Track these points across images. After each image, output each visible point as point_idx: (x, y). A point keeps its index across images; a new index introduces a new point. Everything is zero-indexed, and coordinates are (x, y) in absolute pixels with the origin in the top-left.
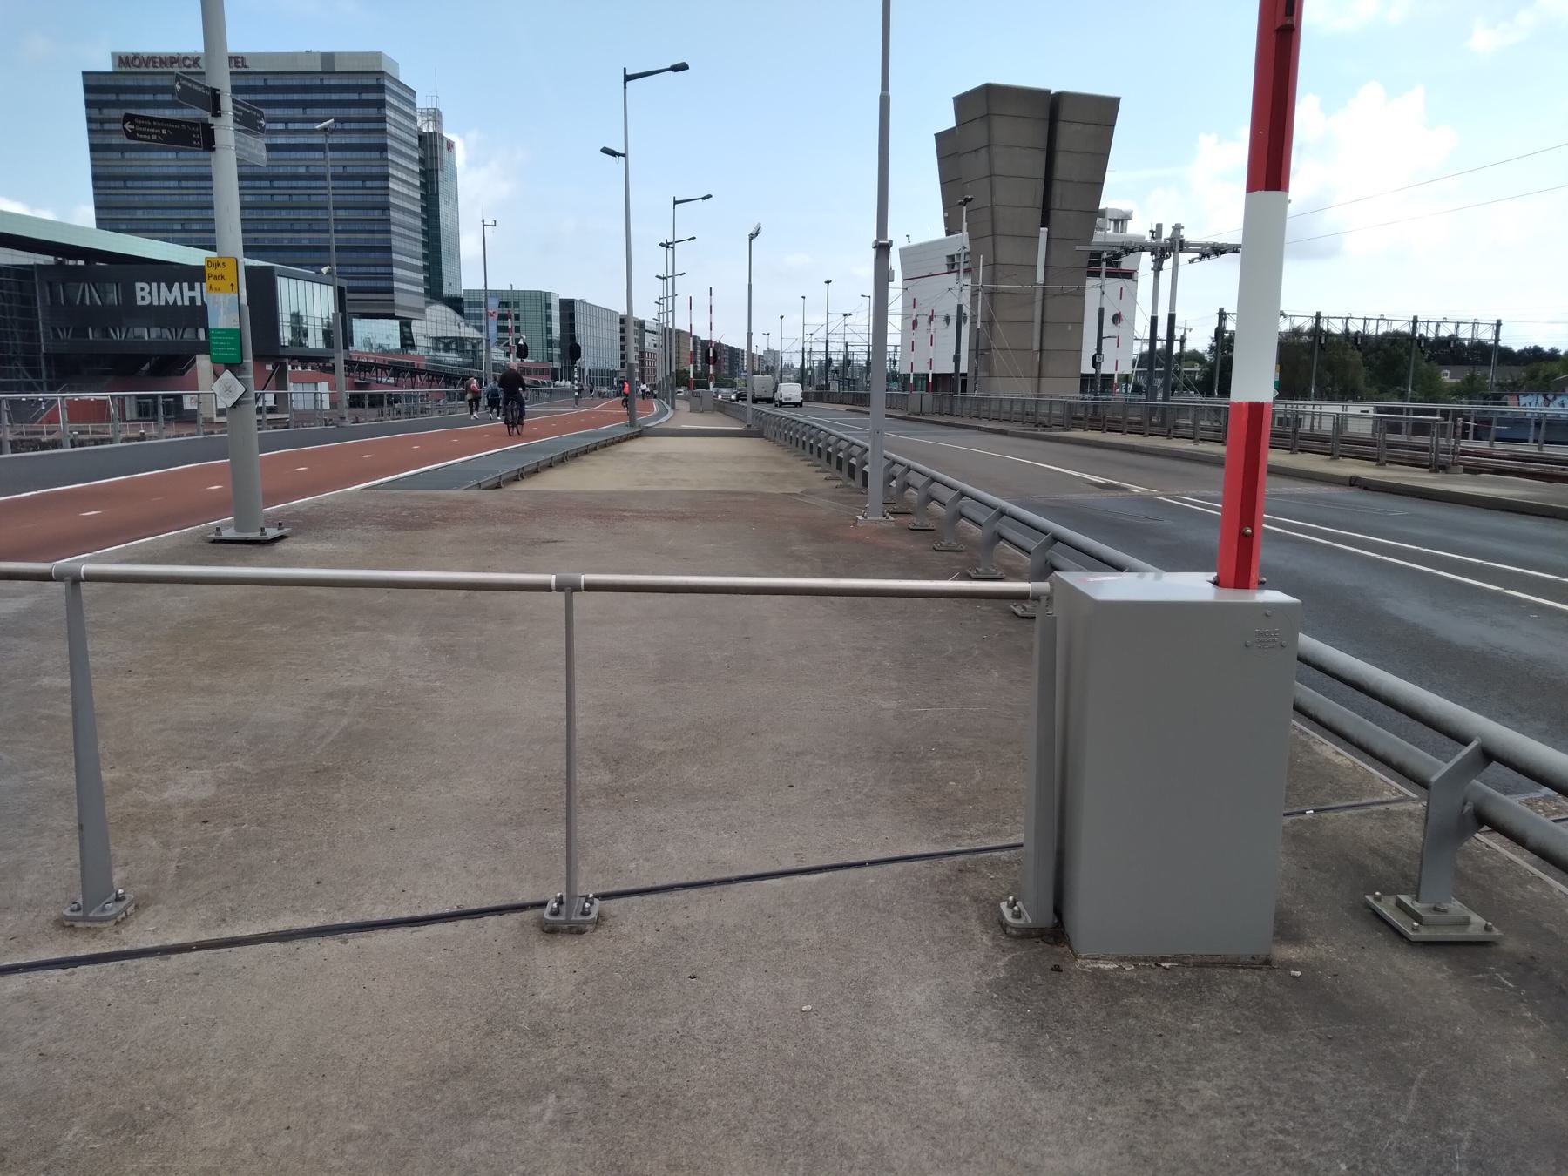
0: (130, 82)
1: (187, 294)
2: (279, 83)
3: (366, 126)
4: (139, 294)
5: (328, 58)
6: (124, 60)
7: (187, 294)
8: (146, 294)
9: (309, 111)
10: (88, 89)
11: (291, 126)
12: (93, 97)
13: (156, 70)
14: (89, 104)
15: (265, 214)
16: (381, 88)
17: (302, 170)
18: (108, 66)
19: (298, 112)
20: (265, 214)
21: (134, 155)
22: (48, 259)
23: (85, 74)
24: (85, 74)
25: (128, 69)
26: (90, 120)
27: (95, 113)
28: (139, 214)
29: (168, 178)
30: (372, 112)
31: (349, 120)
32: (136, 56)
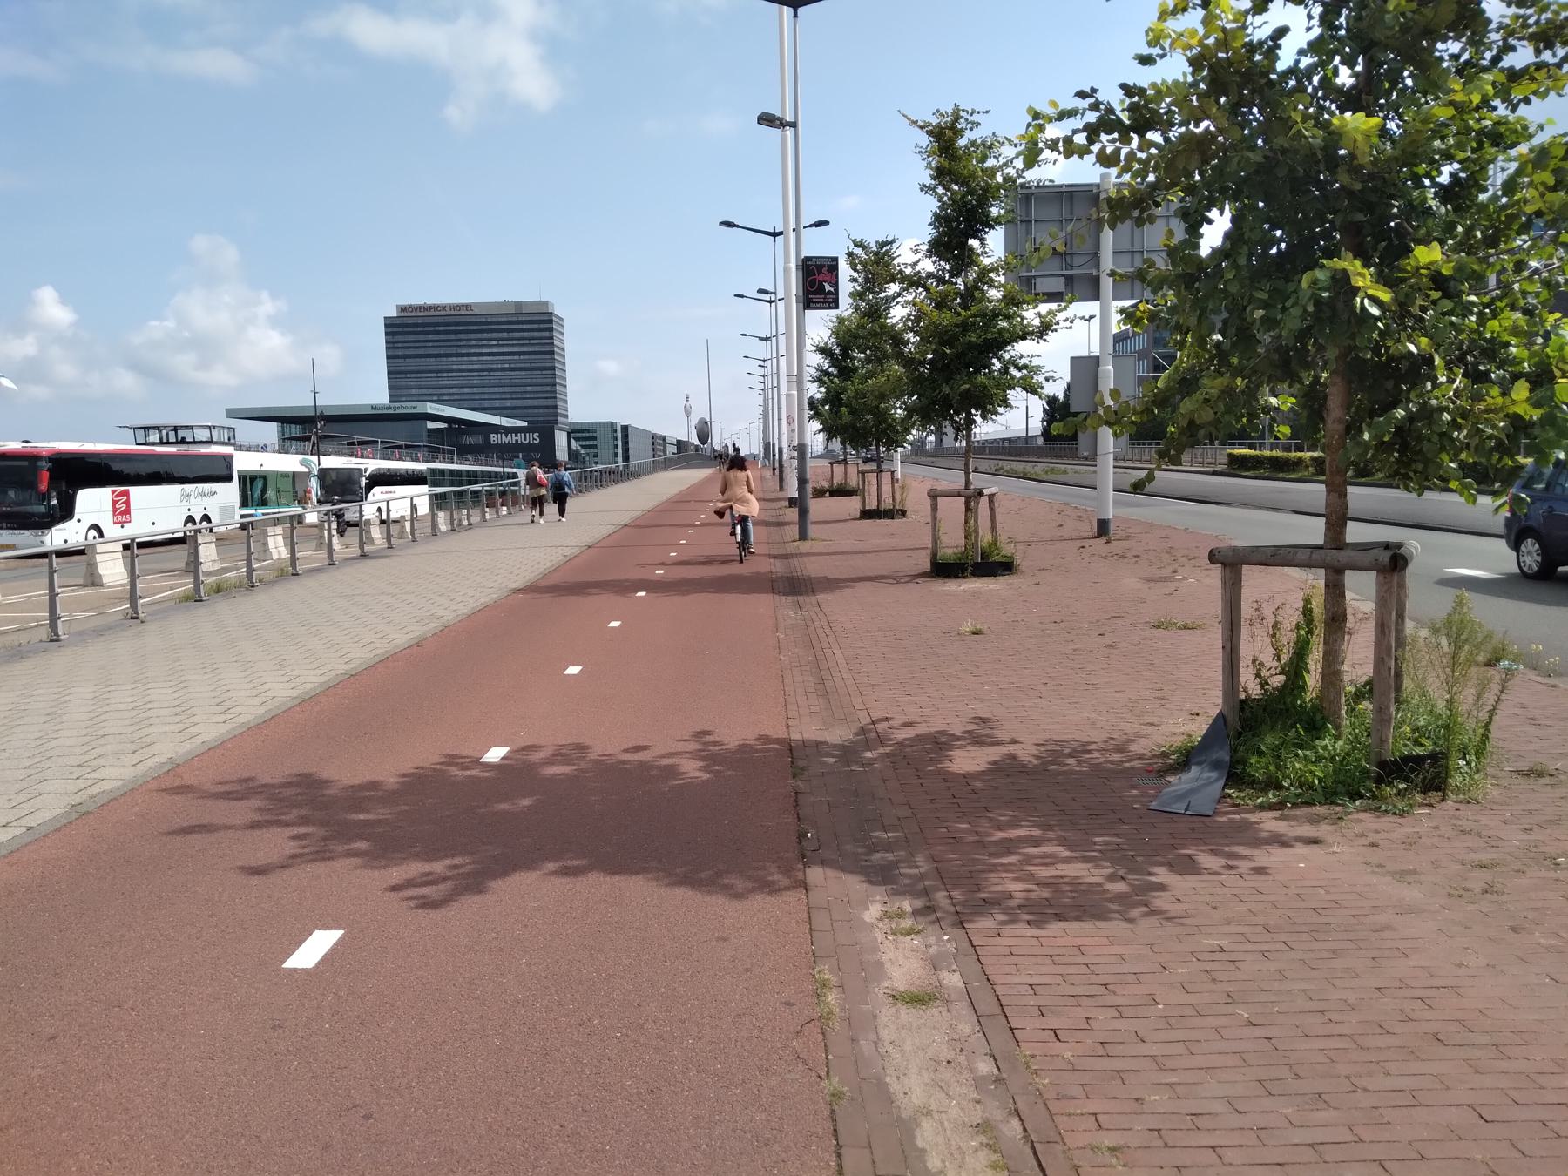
0: (410, 321)
1: (514, 438)
2: (494, 319)
3: (543, 341)
4: (492, 439)
5: (519, 304)
6: (403, 309)
7: (514, 438)
8: (495, 439)
9: (511, 334)
10: (386, 326)
11: (501, 342)
12: (389, 330)
13: (421, 314)
14: (387, 334)
15: (486, 390)
16: (551, 321)
17: (507, 366)
18: (394, 313)
19: (505, 335)
20: (486, 390)
21: (411, 360)
22: (445, 425)
23: (385, 318)
24: (385, 318)
25: (406, 314)
26: (387, 342)
27: (390, 338)
28: (413, 391)
29: (430, 372)
30: (547, 334)
31: (534, 339)
32: (410, 306)
